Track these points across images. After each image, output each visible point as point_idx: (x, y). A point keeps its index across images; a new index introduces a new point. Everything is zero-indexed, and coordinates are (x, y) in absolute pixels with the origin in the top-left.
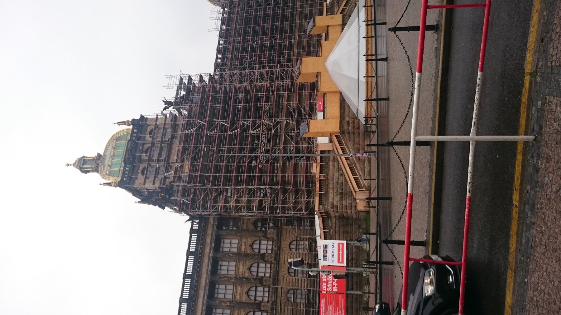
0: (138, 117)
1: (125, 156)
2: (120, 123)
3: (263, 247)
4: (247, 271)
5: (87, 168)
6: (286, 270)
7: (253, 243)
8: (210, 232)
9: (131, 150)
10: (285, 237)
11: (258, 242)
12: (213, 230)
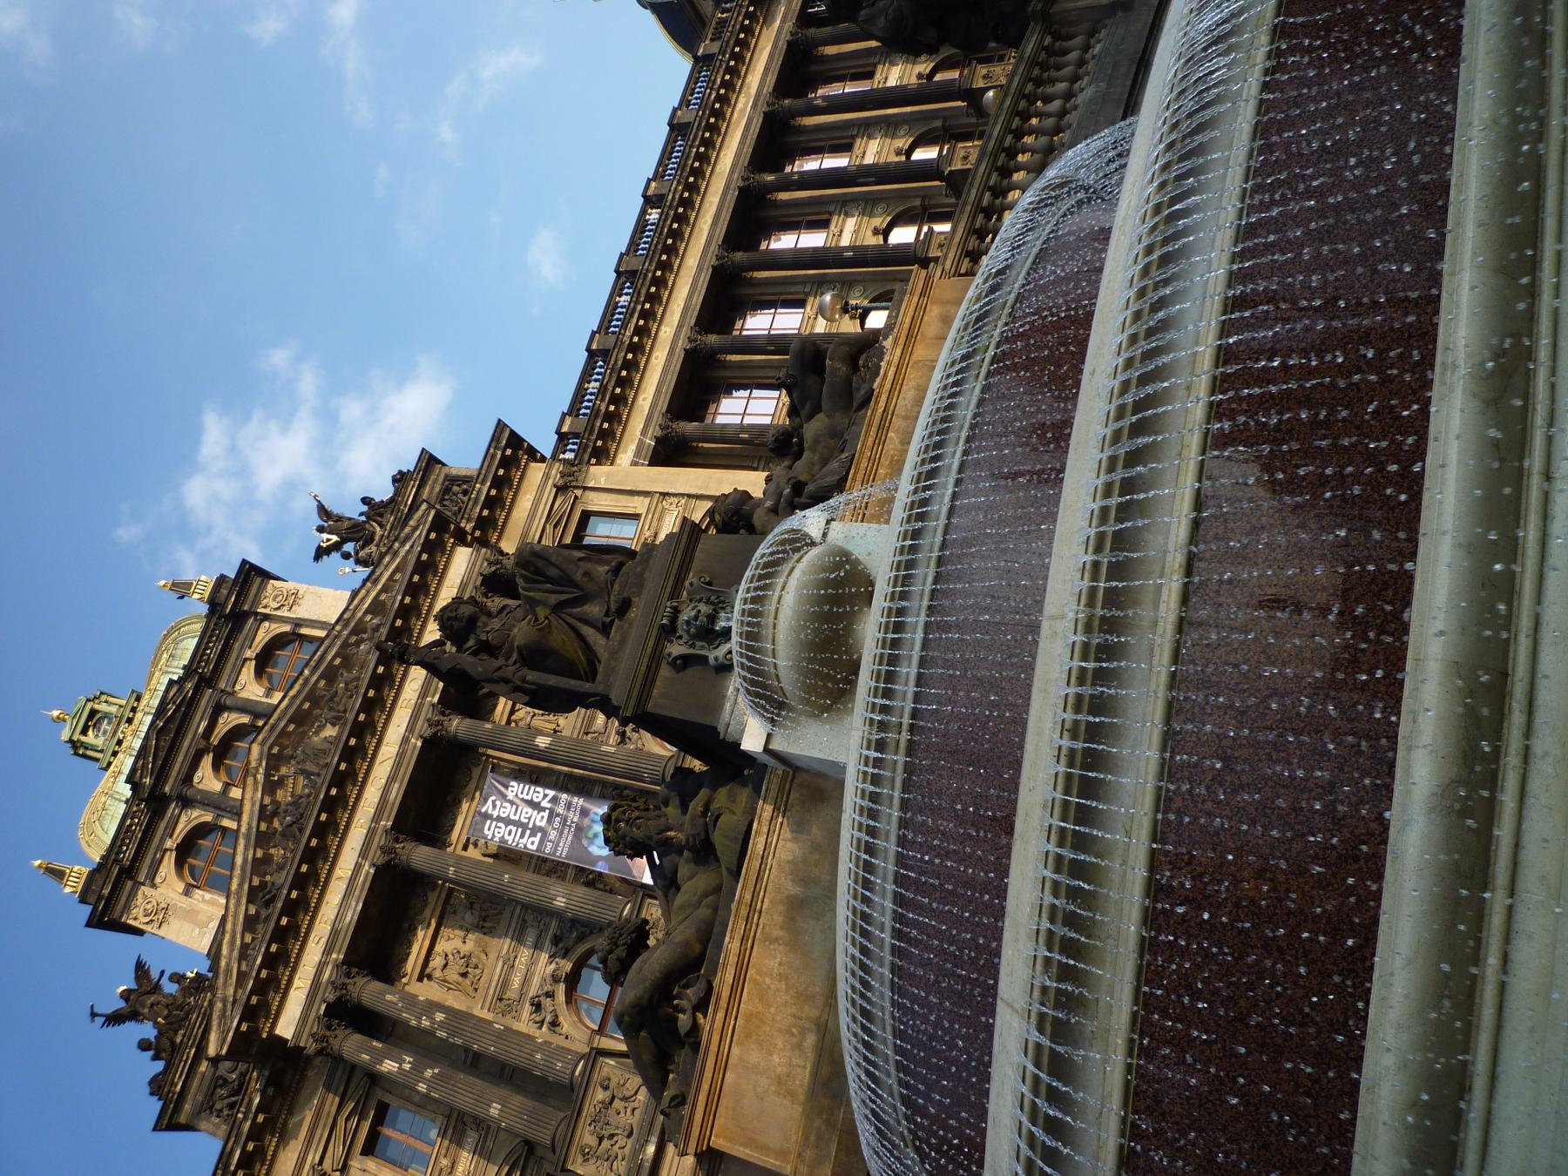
9: (161, 732)
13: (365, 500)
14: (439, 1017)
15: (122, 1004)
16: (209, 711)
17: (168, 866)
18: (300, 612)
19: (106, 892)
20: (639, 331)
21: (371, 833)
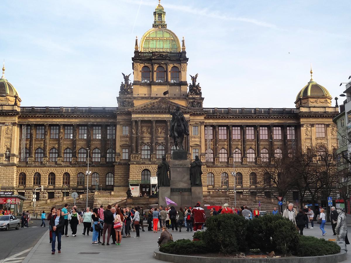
0: (187, 56)
1: (157, 52)
2: (183, 41)
3: (97, 154)
4: (81, 146)
5: (156, 17)
6: (81, 172)
7: (98, 149)
8: (104, 120)
10: (101, 169)
11: (99, 152)
12: (104, 122)
13: (199, 84)
14: (139, 135)
15: (126, 76)
16: (165, 63)
17: (142, 65)
18: (182, 72)
19: (137, 58)
20: (231, 117)
21: (154, 118)
